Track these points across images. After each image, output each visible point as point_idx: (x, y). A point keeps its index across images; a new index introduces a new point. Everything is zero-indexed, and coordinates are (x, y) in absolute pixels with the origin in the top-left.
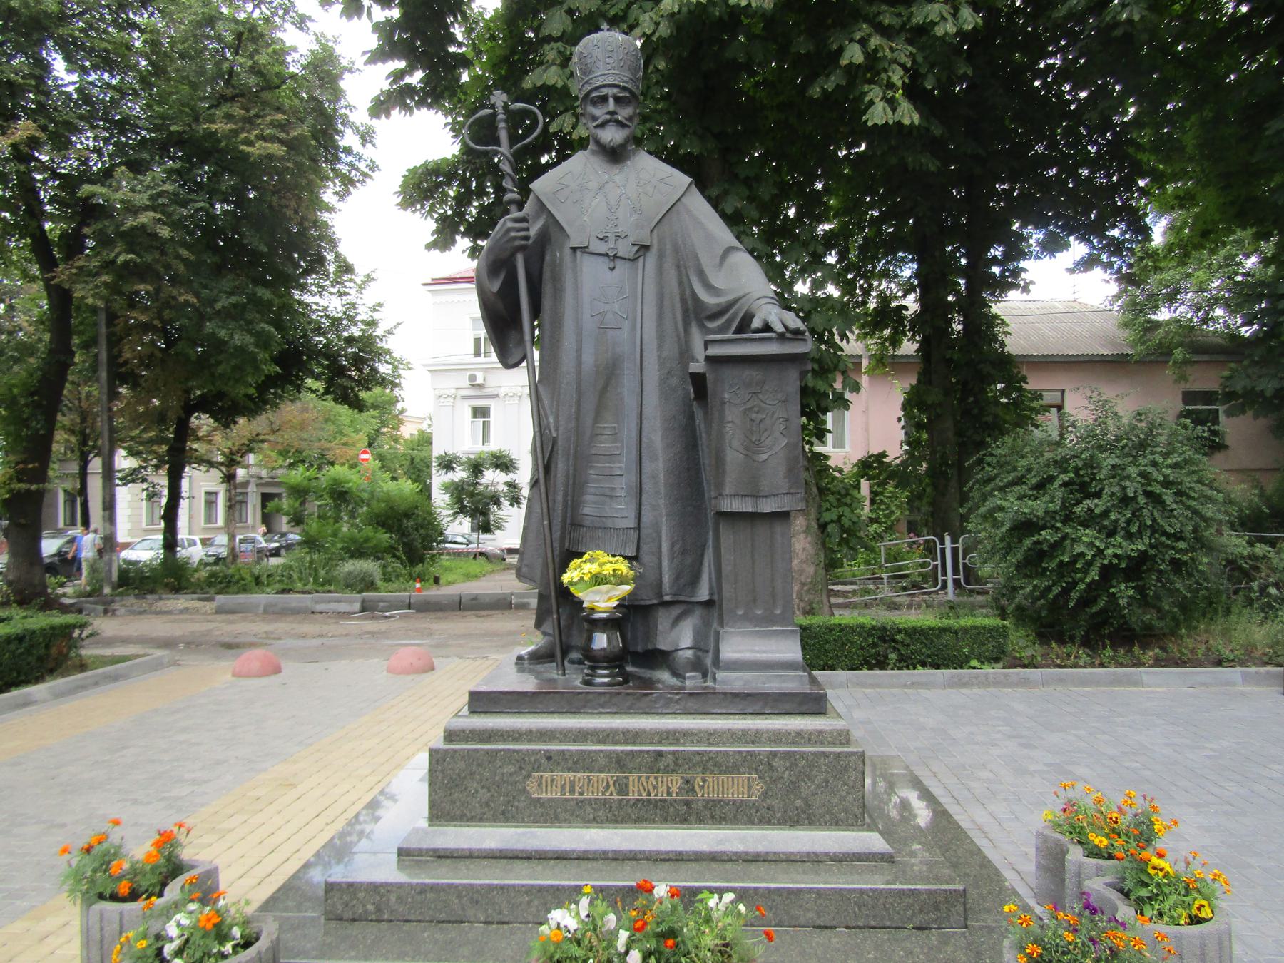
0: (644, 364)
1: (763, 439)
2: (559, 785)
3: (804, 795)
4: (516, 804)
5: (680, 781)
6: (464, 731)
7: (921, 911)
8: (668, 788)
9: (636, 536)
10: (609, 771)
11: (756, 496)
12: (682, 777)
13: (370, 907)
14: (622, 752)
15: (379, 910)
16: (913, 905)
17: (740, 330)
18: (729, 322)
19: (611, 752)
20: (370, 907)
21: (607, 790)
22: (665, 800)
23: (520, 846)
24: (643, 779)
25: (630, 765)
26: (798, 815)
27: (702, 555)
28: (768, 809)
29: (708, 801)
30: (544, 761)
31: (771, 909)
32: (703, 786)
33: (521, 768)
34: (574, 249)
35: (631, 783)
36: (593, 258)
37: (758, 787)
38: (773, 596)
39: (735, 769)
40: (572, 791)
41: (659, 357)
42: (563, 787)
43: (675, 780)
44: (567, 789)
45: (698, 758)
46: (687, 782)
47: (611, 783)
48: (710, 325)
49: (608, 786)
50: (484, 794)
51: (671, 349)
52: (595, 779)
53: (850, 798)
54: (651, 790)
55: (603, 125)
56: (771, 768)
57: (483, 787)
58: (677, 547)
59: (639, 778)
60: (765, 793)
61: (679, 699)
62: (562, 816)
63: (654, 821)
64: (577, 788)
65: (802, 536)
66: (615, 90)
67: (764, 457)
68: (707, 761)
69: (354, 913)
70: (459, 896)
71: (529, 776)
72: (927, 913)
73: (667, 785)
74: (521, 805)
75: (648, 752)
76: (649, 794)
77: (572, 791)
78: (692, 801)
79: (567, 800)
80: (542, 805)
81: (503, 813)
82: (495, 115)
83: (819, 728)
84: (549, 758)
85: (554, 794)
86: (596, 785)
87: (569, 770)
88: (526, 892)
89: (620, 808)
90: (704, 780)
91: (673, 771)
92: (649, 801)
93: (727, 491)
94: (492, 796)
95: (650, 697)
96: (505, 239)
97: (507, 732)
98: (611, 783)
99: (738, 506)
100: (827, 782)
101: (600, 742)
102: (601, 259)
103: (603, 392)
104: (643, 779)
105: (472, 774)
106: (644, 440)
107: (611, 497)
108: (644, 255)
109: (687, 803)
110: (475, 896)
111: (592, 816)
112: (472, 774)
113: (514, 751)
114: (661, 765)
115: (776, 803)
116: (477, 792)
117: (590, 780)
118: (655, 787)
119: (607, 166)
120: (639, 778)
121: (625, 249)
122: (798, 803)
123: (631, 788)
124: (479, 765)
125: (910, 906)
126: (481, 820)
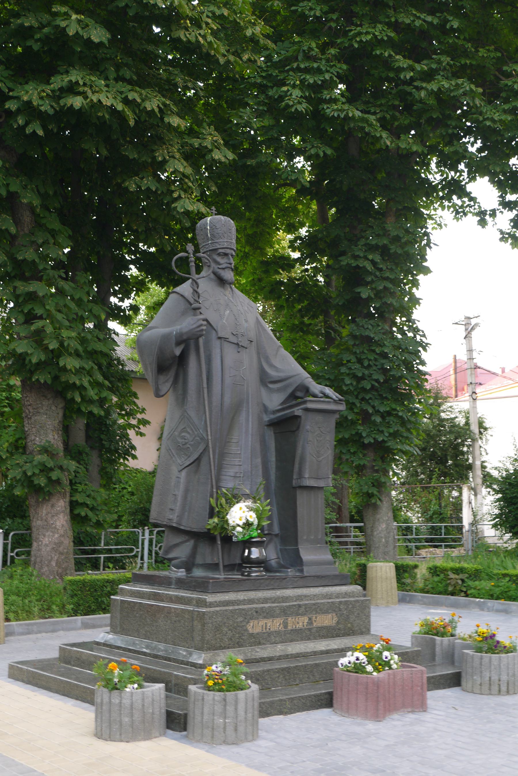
6: (216, 602)
11: (317, 478)
14: (286, 606)
19: (282, 607)
23: (253, 657)
25: (289, 613)
30: (255, 614)
36: (229, 344)
37: (335, 619)
39: (326, 612)
40: (266, 628)
43: (305, 620)
45: (314, 607)
48: (271, 386)
50: (230, 634)
55: (223, 269)
56: (340, 610)
57: (230, 630)
60: (338, 622)
62: (262, 641)
63: (298, 641)
64: (268, 627)
65: (61, 516)
71: (248, 622)
73: (302, 622)
75: (295, 605)
77: (266, 628)
78: (311, 629)
79: (264, 633)
81: (238, 643)
82: (187, 258)
84: (257, 612)
85: (257, 630)
87: (265, 617)
88: (278, 672)
89: (285, 635)
90: (316, 618)
91: (305, 614)
93: (307, 476)
95: (285, 581)
96: (198, 329)
100: (358, 614)
101: (273, 603)
102: (234, 345)
103: (233, 418)
105: (225, 623)
107: (235, 477)
109: (310, 630)
112: (225, 623)
113: (243, 610)
114: (300, 612)
115: (341, 626)
116: (227, 633)
119: (222, 290)
122: (349, 625)
124: (228, 618)
126: (228, 648)
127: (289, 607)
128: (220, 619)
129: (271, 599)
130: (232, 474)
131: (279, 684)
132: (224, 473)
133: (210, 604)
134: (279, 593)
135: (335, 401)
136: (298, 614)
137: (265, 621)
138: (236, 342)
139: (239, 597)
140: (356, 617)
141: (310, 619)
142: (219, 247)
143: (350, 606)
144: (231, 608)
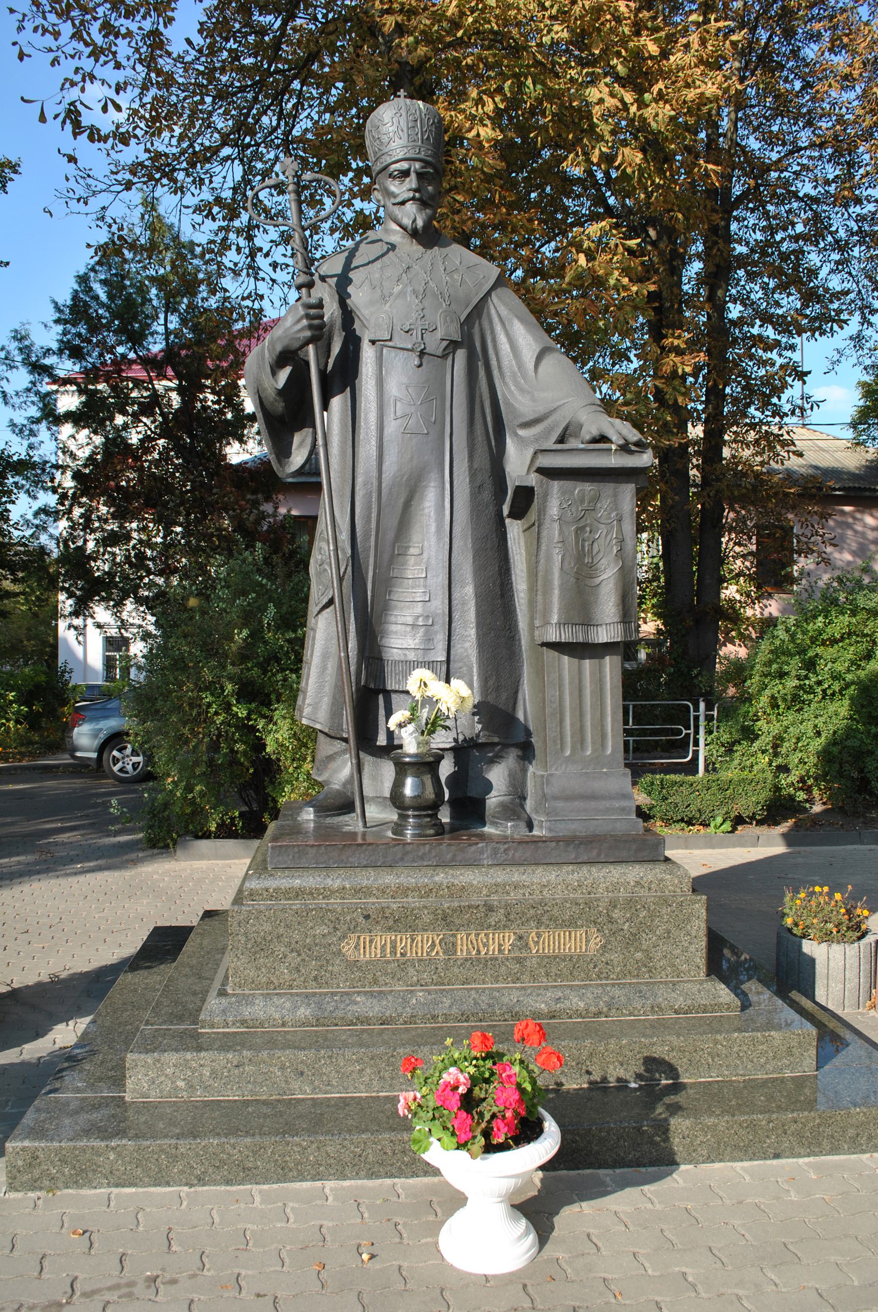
0: (455, 475)
1: (595, 561)
2: (379, 947)
3: (644, 947)
4: (330, 968)
5: (513, 937)
7: (774, 1058)
8: (500, 945)
9: (444, 668)
10: (434, 930)
12: (515, 933)
13: (181, 1084)
15: (191, 1087)
16: (766, 1052)
17: (561, 440)
18: (550, 430)
20: (181, 1084)
21: (432, 950)
22: (496, 959)
23: (339, 1013)
24: (473, 936)
25: (457, 921)
26: (639, 969)
27: (516, 692)
28: (607, 963)
29: (542, 958)
30: (361, 919)
31: (622, 1065)
32: (537, 943)
33: (336, 929)
34: (373, 342)
35: (459, 942)
36: (393, 352)
37: (596, 941)
38: (603, 736)
39: (571, 924)
40: (394, 952)
41: (471, 468)
42: (383, 947)
43: (509, 939)
44: (388, 951)
45: (532, 911)
46: (521, 938)
47: (437, 942)
49: (433, 945)
51: (483, 459)
52: (420, 938)
53: (692, 949)
54: (481, 948)
55: (403, 203)
56: (611, 921)
57: (292, 951)
58: (491, 683)
59: (468, 935)
60: (604, 946)
61: (505, 850)
66: (418, 165)
67: (597, 581)
68: (542, 915)
69: (161, 1091)
70: (282, 1068)
71: (345, 937)
72: (780, 1059)
74: (336, 969)
76: (479, 952)
77: (394, 952)
78: (525, 959)
79: (388, 962)
80: (360, 969)
81: (315, 979)
83: (659, 876)
84: (367, 917)
85: (372, 953)
86: (420, 945)
87: (390, 929)
90: (539, 936)
91: (505, 926)
92: (478, 960)
94: (303, 960)
97: (316, 889)
98: (437, 942)
99: (566, 636)
104: (473, 936)
106: (453, 562)
108: (454, 353)
109: (519, 961)
110: (301, 1067)
111: (415, 978)
114: (492, 921)
116: (285, 957)
117: (413, 940)
118: (485, 945)
120: (468, 935)
121: (435, 343)
122: (639, 955)
123: (459, 947)
125: (763, 1053)
127: (461, 910)
128: (267, 927)
129: (417, 889)
130: (410, 620)
131: (362, 1087)
132: (393, 619)
133: (251, 895)
134: (441, 877)
135: (625, 448)
136: (483, 925)
137: (390, 937)
138: (410, 347)
139: (329, 882)
140: (659, 938)
141: (521, 938)
142: (389, 161)
143: (643, 914)
144: (297, 904)
